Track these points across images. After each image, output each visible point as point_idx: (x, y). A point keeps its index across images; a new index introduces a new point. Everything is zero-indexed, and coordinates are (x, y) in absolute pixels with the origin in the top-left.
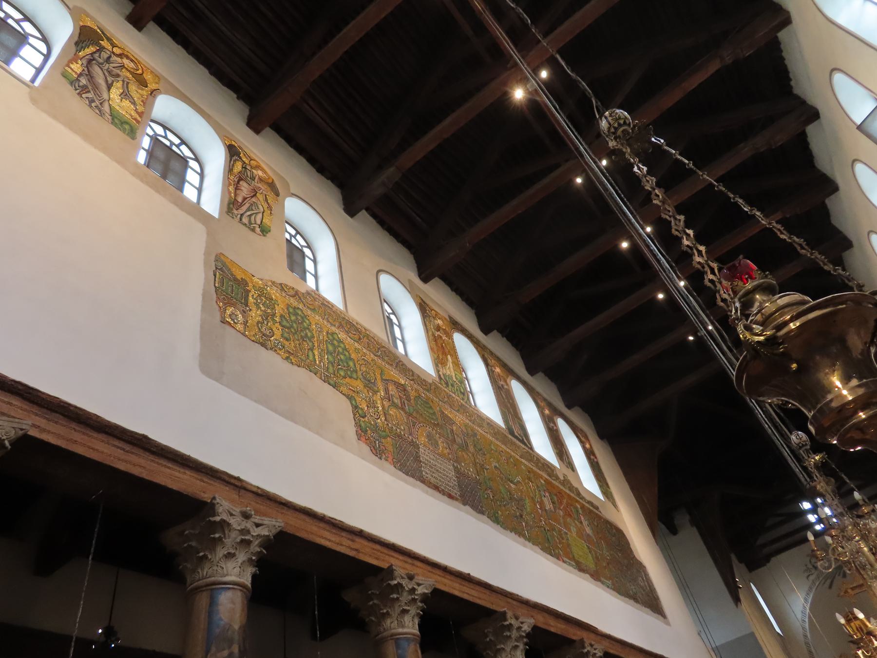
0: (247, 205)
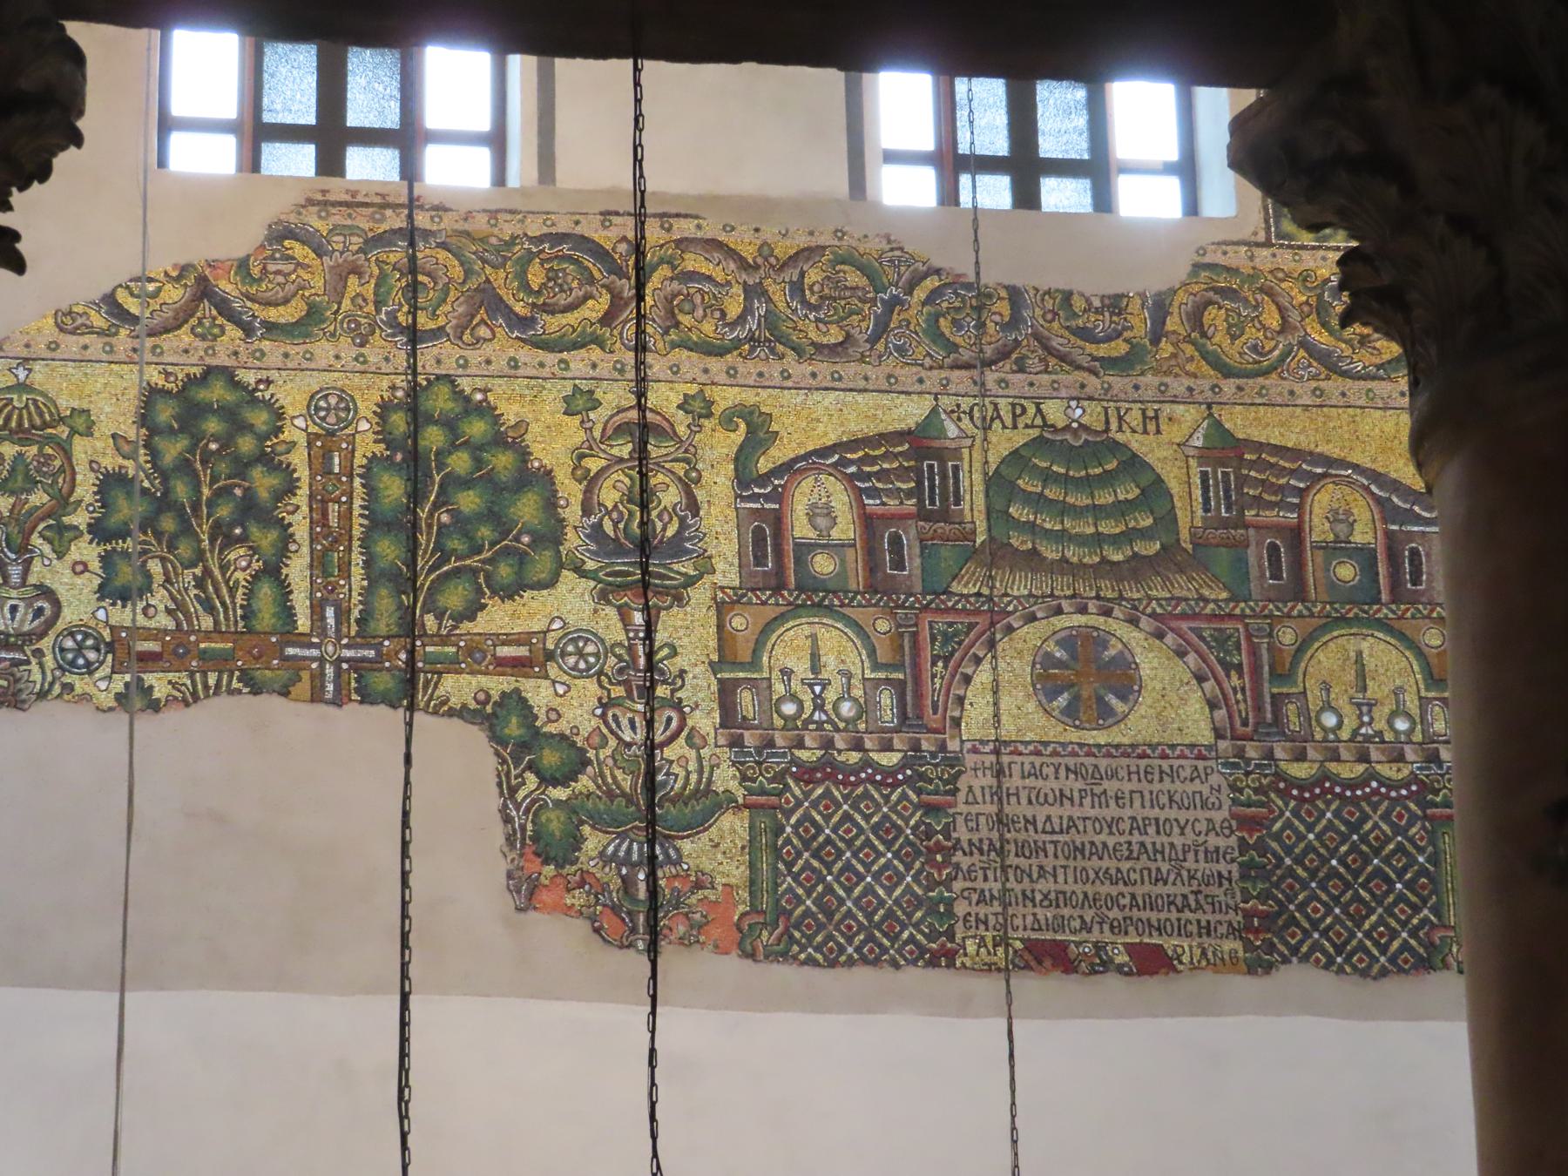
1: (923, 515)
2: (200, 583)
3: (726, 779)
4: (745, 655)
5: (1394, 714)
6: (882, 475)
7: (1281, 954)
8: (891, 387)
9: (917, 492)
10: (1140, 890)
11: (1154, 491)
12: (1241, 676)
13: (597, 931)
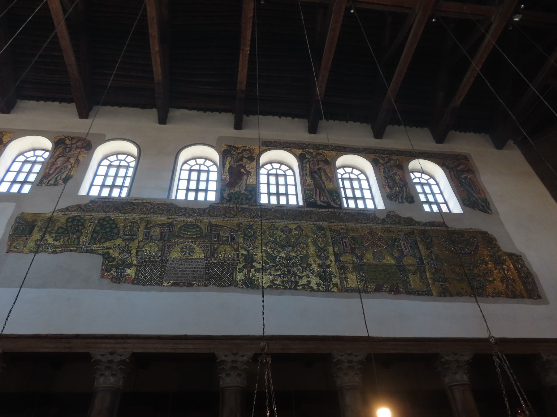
0: (58, 171)
1: (169, 232)
2: (68, 239)
3: (135, 262)
4: (141, 247)
5: (229, 255)
6: (165, 227)
7: (209, 284)
9: (169, 229)
10: (190, 276)
12: (209, 250)
13: (112, 281)
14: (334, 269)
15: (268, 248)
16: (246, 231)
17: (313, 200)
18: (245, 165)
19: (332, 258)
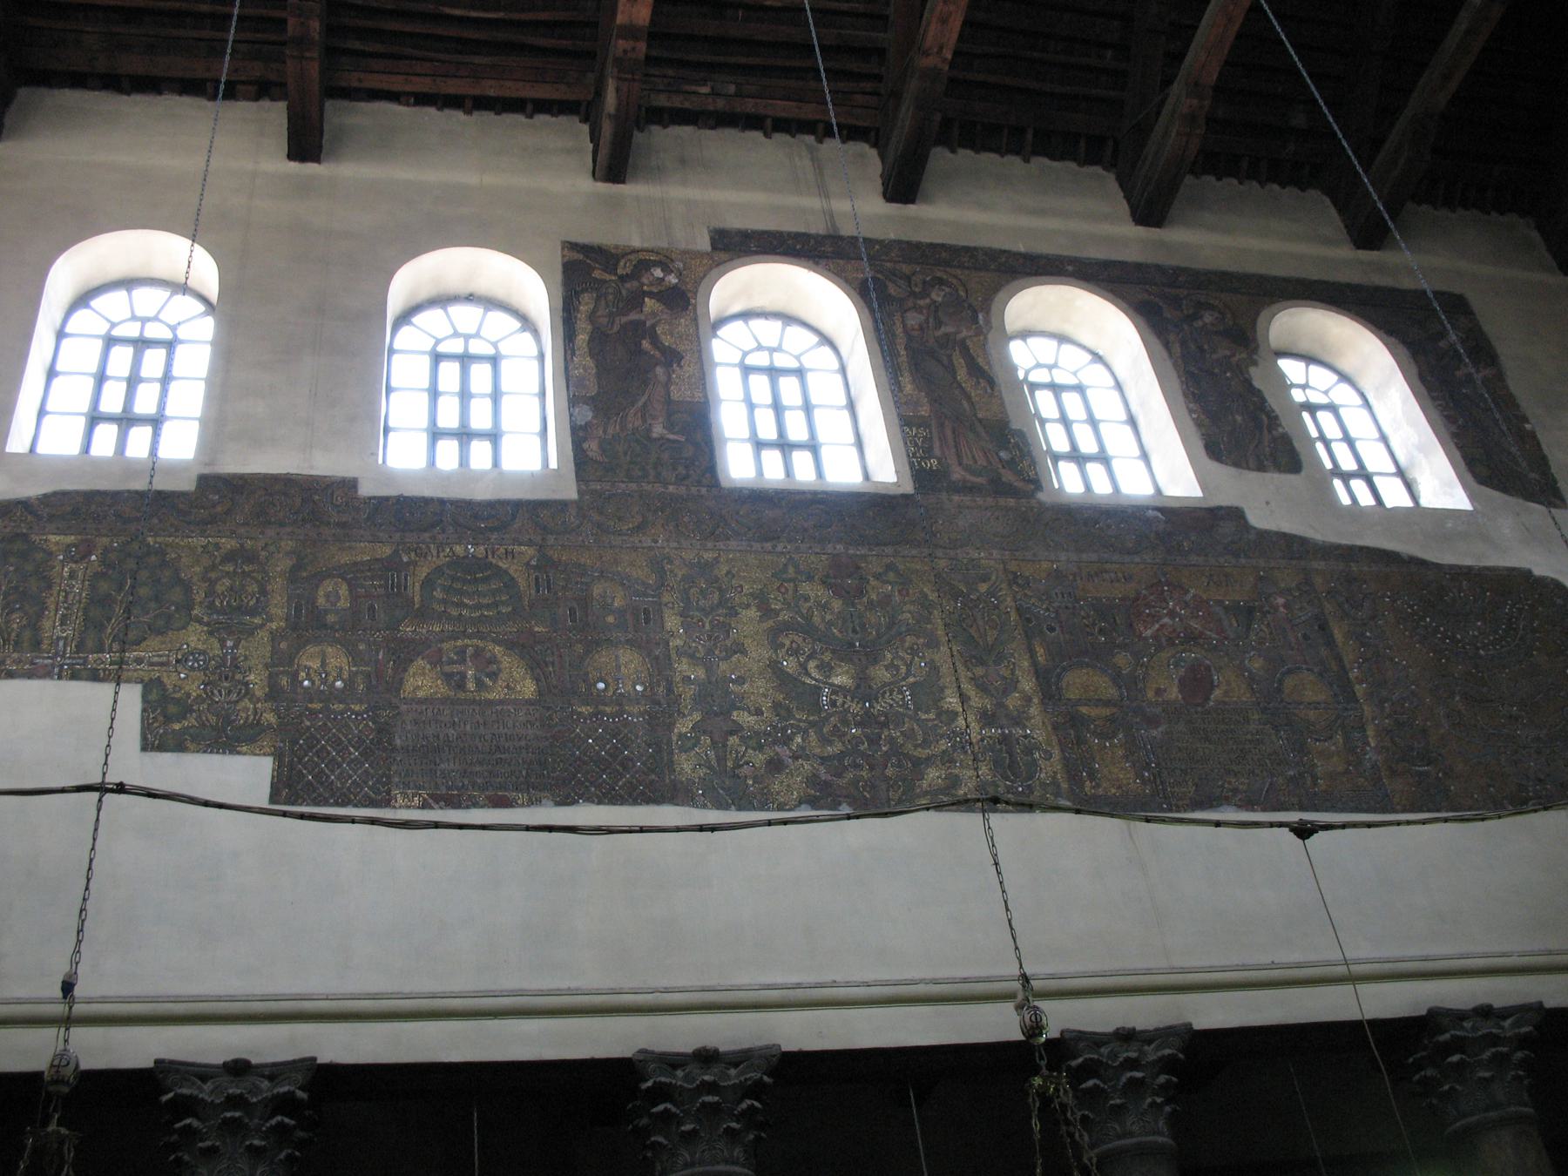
8: (376, 540)
11: (511, 584)
14: (1037, 727)
15: (781, 653)
16: (691, 587)
17: (934, 462)
18: (653, 327)
19: (1027, 684)
